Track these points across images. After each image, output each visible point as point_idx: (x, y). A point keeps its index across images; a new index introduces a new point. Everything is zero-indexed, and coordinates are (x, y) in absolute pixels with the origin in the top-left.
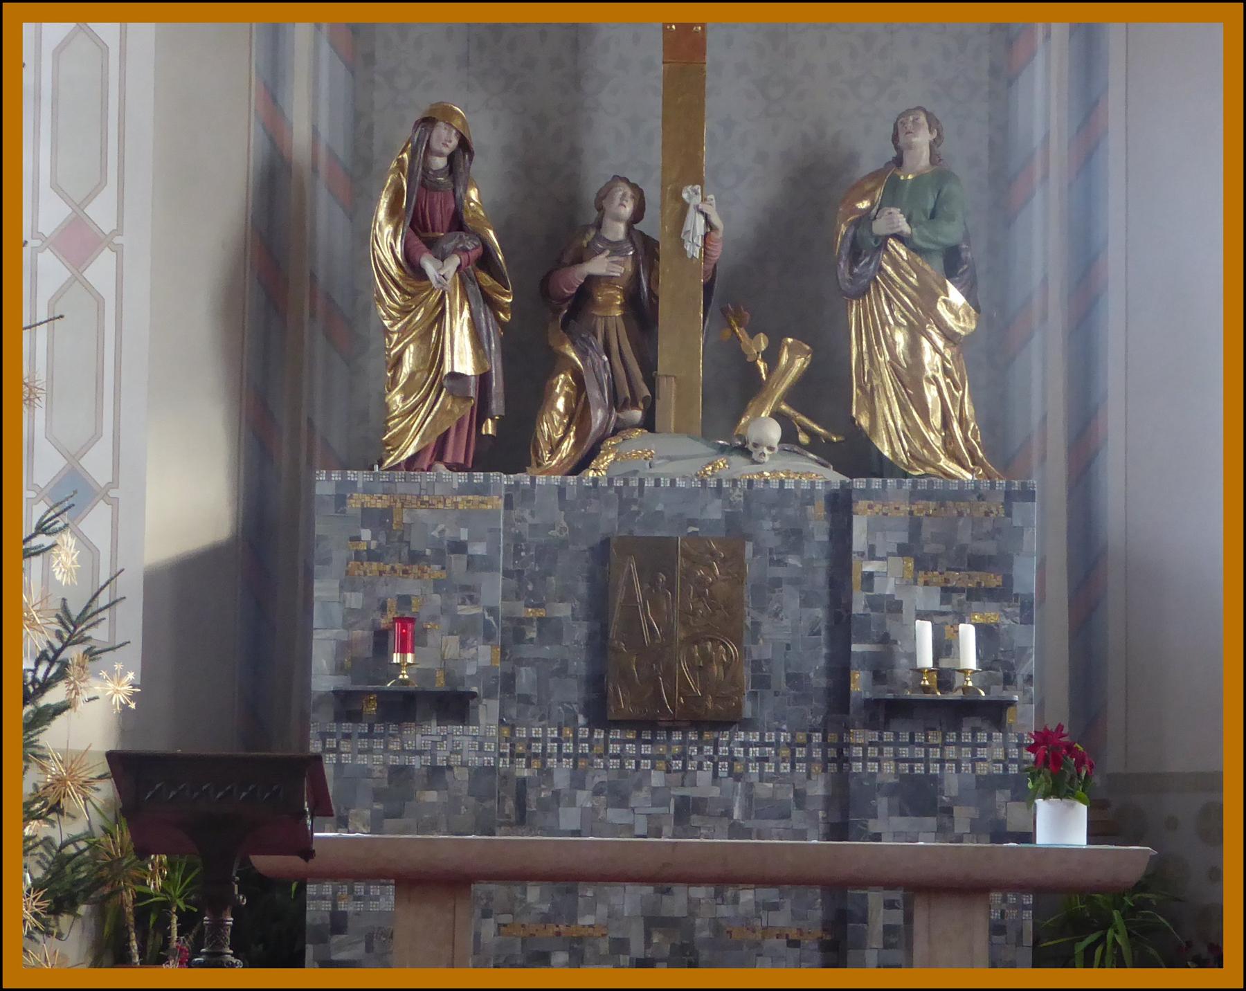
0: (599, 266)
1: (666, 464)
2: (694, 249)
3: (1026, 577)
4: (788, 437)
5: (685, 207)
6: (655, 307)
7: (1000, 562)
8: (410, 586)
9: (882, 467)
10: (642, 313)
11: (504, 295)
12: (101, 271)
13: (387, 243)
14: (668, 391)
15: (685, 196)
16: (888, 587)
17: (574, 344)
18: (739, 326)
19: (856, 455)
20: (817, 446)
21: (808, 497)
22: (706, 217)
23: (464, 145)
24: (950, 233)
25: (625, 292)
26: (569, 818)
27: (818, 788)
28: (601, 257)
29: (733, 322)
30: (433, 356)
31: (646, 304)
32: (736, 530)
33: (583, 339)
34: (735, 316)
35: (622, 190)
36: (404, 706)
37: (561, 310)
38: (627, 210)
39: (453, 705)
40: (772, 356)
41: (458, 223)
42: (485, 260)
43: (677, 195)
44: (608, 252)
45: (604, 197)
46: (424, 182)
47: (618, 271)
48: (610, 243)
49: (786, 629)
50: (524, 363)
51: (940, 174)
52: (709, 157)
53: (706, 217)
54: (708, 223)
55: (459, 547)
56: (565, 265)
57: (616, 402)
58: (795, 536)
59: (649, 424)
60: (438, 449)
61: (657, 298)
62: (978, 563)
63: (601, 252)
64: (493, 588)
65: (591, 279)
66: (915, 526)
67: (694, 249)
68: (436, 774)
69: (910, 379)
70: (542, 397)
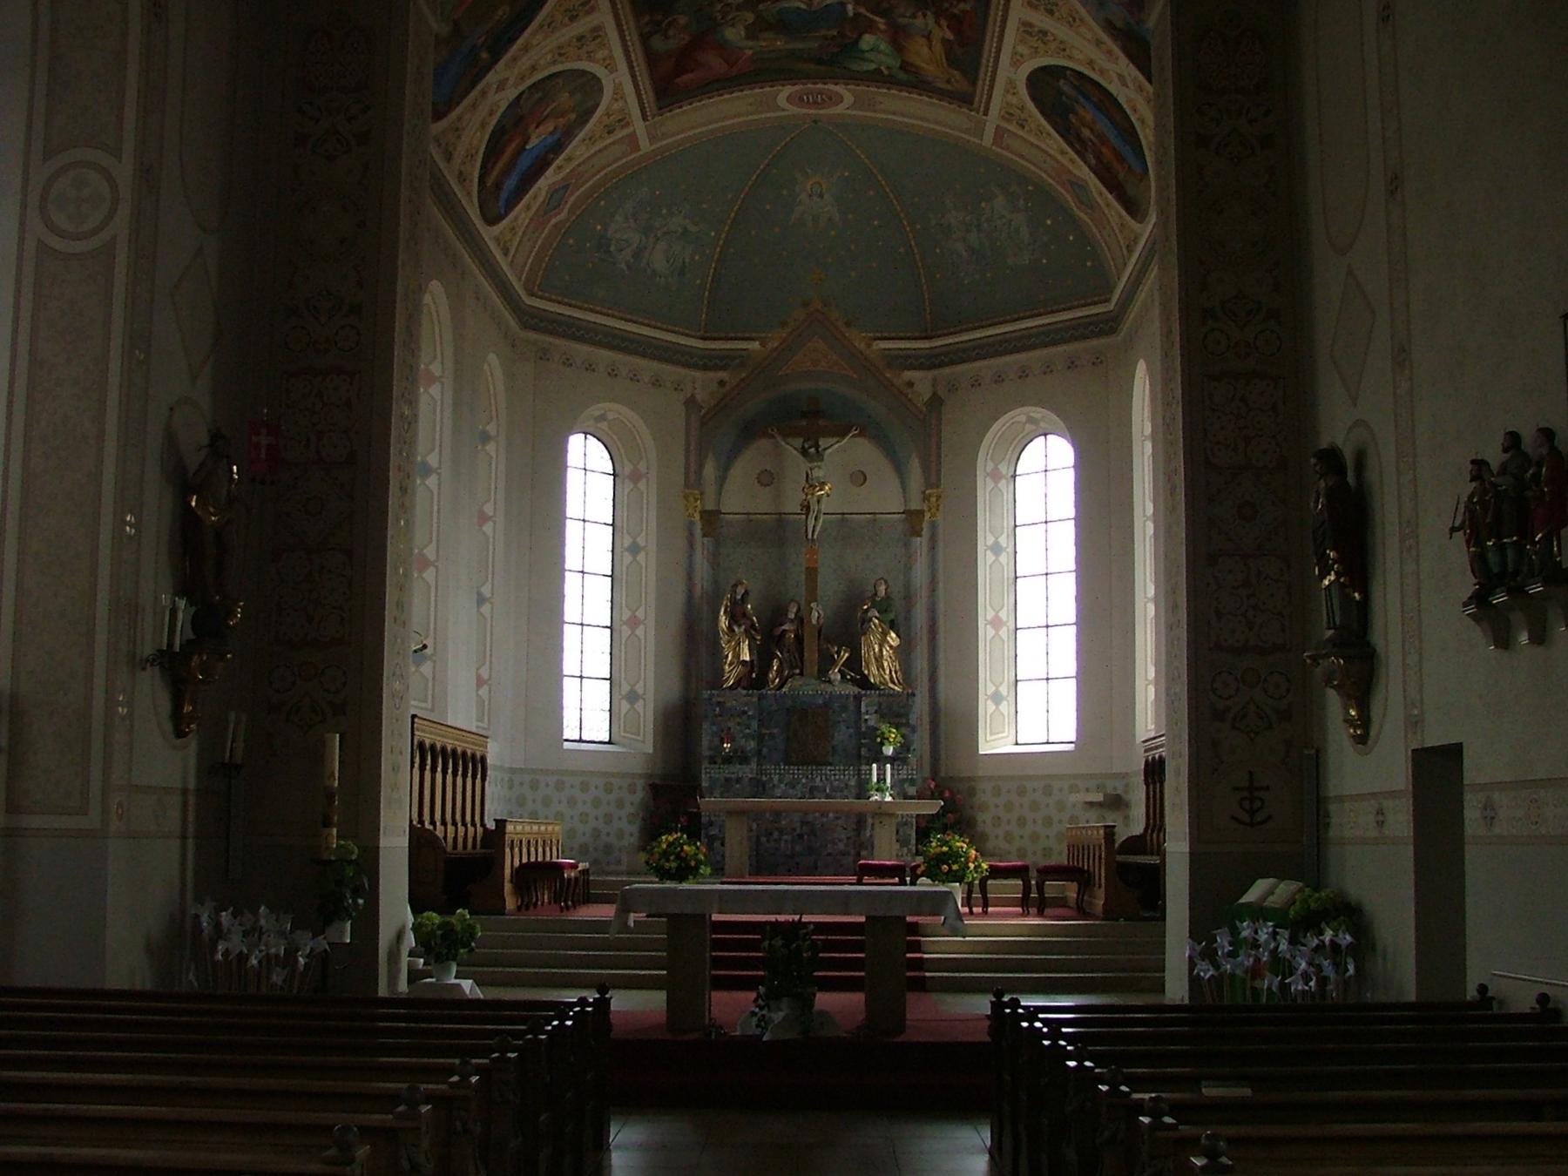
0: (785, 627)
1: (806, 687)
2: (814, 622)
3: (913, 719)
4: (843, 677)
7: (906, 715)
8: (730, 724)
9: (872, 687)
10: (799, 639)
12: (640, 631)
13: (723, 622)
14: (807, 664)
16: (871, 723)
19: (864, 683)
20: (853, 680)
21: (848, 696)
23: (746, 592)
24: (892, 616)
26: (778, 792)
27: (852, 783)
30: (737, 655)
32: (826, 705)
36: (728, 760)
39: (744, 760)
40: (838, 653)
41: (744, 615)
42: (753, 625)
46: (733, 601)
49: (842, 735)
50: (763, 656)
51: (888, 597)
52: (819, 592)
55: (745, 713)
57: (792, 668)
58: (844, 708)
59: (801, 674)
60: (737, 683)
62: (899, 715)
64: (755, 724)
66: (880, 704)
67: (814, 622)
68: (739, 780)
69: (879, 659)
70: (770, 666)
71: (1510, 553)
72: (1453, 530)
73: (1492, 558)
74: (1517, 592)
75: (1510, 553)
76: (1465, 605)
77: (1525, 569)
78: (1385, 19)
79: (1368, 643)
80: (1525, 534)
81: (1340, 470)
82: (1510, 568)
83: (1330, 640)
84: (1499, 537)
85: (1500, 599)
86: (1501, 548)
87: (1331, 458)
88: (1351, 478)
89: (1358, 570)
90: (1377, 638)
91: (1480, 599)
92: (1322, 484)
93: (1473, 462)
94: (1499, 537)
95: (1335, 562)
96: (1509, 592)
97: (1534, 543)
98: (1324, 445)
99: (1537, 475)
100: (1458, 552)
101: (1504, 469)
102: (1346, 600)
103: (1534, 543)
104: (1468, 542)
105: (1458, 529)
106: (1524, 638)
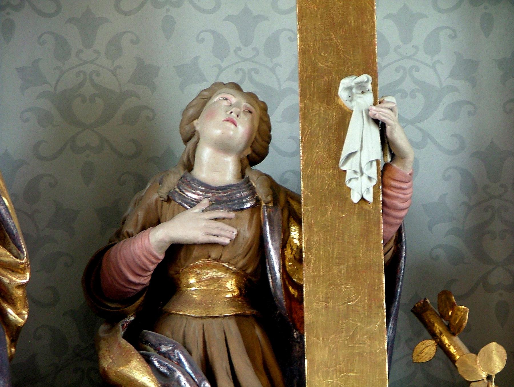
2: (361, 186)
5: (344, 117)
6: (297, 302)
10: (272, 315)
11: (13, 268)
15: (342, 94)
17: (148, 360)
18: (452, 330)
22: (382, 127)
25: (240, 275)
28: (197, 209)
29: (438, 328)
31: (280, 293)
33: (165, 355)
34: (442, 316)
35: (225, 103)
37: (125, 315)
38: (240, 132)
43: (329, 93)
44: (205, 203)
45: (197, 116)
47: (225, 234)
48: (209, 189)
53: (382, 127)
54: (386, 142)
56: (130, 235)
61: (299, 288)
63: (193, 204)
65: (176, 251)
67: (361, 186)
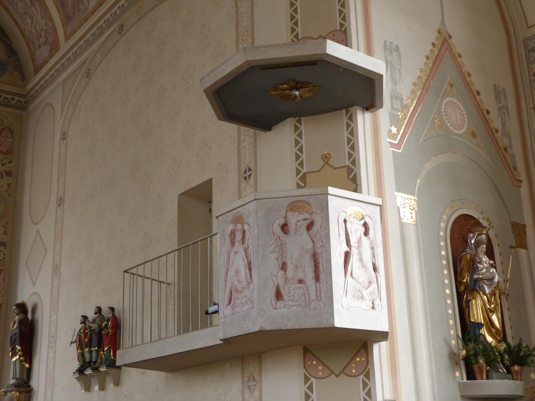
71: (94, 354)
72: (72, 342)
73: (87, 356)
74: (96, 369)
75: (94, 354)
76: (74, 373)
77: (99, 361)
78: (64, 138)
79: (29, 386)
80: (100, 346)
81: (25, 312)
82: (94, 360)
83: (13, 384)
84: (90, 347)
85: (88, 372)
86: (91, 352)
87: (22, 308)
88: (30, 316)
89: (28, 354)
90: (34, 383)
91: (81, 371)
92: (17, 317)
93: (82, 316)
94: (90, 347)
95: (19, 351)
96: (93, 369)
97: (104, 351)
98: (19, 301)
99: (106, 325)
100: (73, 352)
101: (94, 322)
102: (22, 366)
103: (104, 351)
104: (77, 348)
105: (74, 342)
106: (96, 388)
